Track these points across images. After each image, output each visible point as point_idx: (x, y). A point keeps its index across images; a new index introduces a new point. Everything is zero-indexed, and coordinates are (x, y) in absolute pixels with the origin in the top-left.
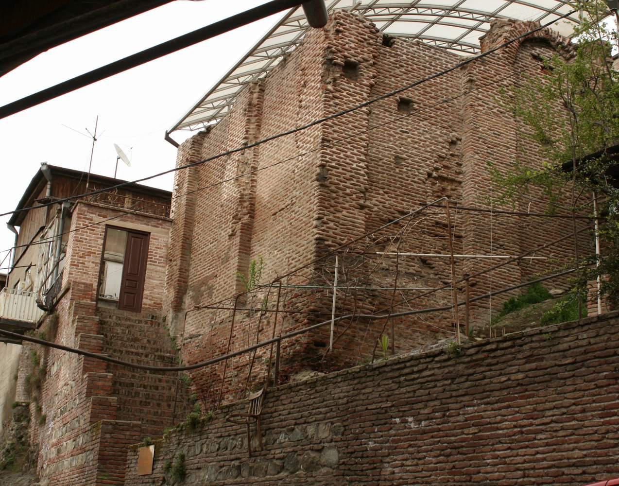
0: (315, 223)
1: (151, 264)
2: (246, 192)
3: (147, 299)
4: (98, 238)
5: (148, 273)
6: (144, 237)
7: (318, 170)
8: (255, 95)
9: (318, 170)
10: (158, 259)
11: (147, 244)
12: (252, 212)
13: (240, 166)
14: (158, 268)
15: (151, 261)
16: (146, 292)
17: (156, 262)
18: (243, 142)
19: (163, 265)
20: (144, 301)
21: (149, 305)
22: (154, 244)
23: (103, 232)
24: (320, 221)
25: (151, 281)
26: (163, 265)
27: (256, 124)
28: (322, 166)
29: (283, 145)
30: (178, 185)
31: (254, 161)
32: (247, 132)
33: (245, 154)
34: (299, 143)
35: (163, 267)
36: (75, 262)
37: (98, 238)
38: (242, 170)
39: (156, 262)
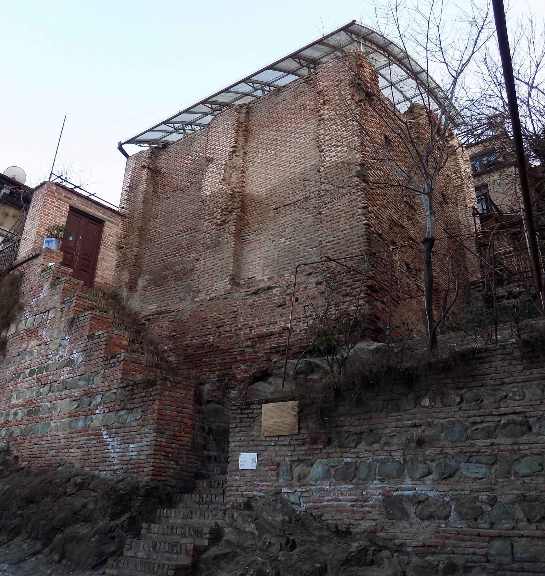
0: (360, 211)
1: (103, 248)
2: (237, 190)
3: (98, 277)
4: (63, 216)
5: (100, 256)
6: (99, 224)
7: (359, 168)
8: (243, 115)
9: (359, 168)
10: (110, 245)
11: (101, 230)
12: (243, 207)
13: (228, 169)
14: (109, 253)
15: (104, 246)
16: (98, 272)
17: (108, 247)
18: (232, 149)
19: (114, 251)
20: (97, 279)
21: (100, 284)
22: (107, 232)
23: (66, 211)
24: (366, 210)
25: (103, 263)
26: (114, 251)
27: (244, 137)
28: (362, 165)
29: (284, 153)
30: (129, 187)
31: (243, 166)
32: (236, 141)
33: (233, 160)
34: (323, 147)
35: (113, 253)
36: (40, 233)
37: (63, 216)
38: (231, 172)
39: (108, 247)
